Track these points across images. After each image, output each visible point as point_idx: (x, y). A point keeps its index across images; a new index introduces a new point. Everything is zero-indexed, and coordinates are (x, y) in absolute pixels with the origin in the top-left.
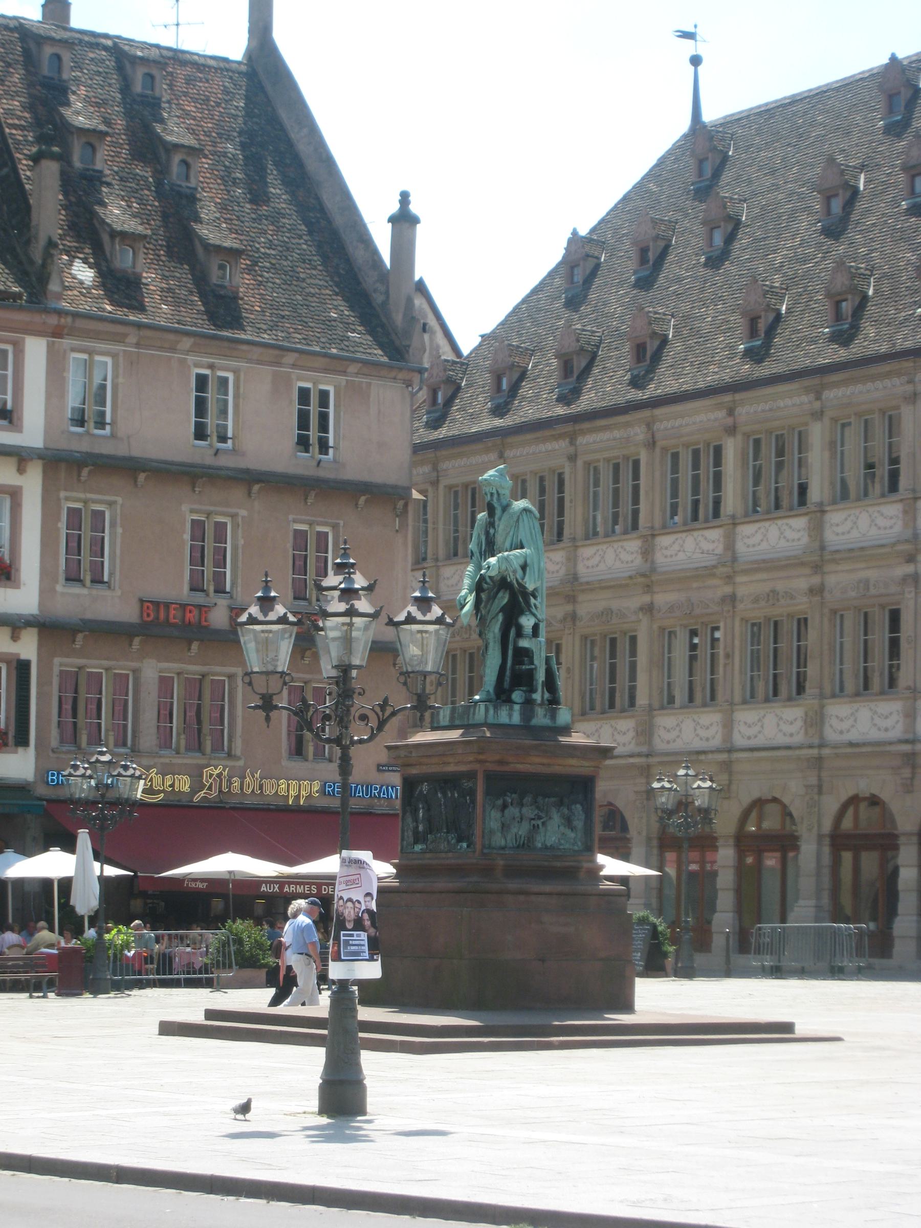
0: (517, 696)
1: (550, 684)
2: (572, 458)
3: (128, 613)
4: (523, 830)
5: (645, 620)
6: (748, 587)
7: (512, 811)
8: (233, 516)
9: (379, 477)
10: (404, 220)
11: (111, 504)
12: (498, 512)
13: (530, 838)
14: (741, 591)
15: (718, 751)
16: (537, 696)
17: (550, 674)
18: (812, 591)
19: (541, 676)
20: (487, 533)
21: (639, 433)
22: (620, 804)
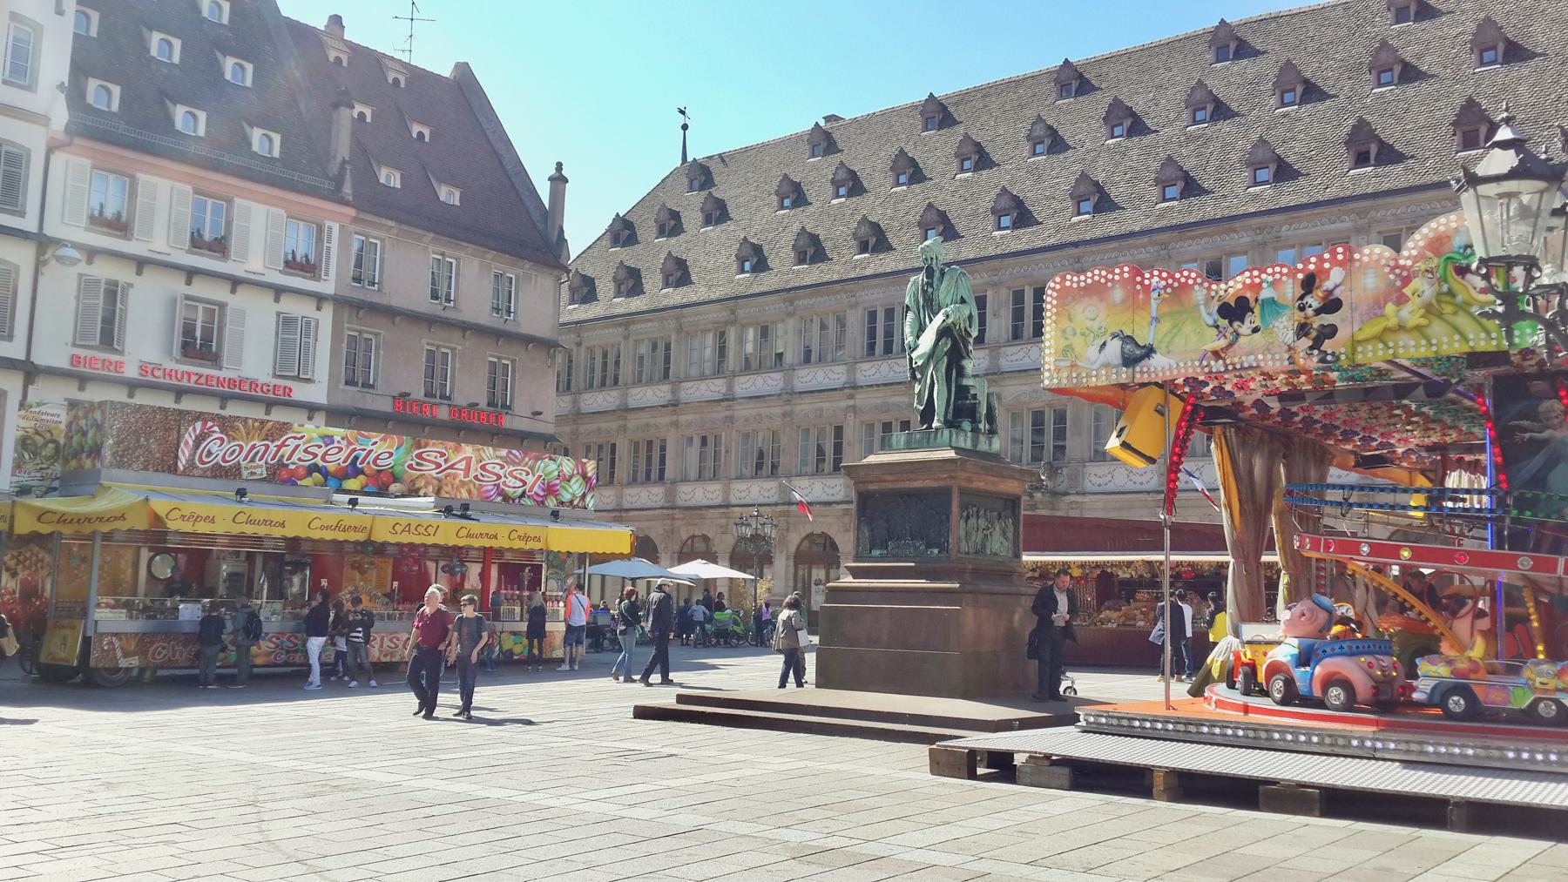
0: (966, 425)
1: (990, 417)
2: (626, 338)
3: (385, 406)
4: (977, 538)
5: (672, 430)
6: (742, 411)
7: (972, 521)
8: (453, 349)
9: (538, 334)
10: (559, 180)
11: (376, 335)
12: (937, 274)
13: (984, 546)
14: (737, 414)
15: (720, 506)
16: (981, 426)
17: (990, 409)
18: (784, 415)
19: (983, 410)
20: (925, 292)
21: (672, 324)
22: (653, 536)
